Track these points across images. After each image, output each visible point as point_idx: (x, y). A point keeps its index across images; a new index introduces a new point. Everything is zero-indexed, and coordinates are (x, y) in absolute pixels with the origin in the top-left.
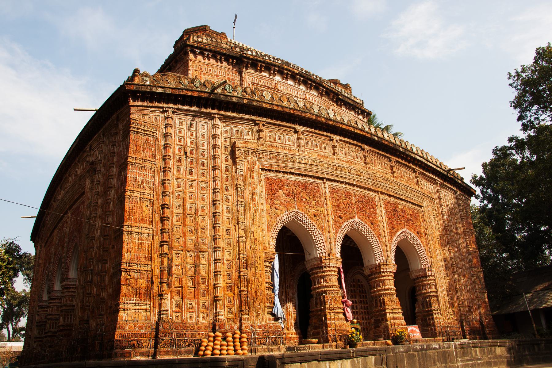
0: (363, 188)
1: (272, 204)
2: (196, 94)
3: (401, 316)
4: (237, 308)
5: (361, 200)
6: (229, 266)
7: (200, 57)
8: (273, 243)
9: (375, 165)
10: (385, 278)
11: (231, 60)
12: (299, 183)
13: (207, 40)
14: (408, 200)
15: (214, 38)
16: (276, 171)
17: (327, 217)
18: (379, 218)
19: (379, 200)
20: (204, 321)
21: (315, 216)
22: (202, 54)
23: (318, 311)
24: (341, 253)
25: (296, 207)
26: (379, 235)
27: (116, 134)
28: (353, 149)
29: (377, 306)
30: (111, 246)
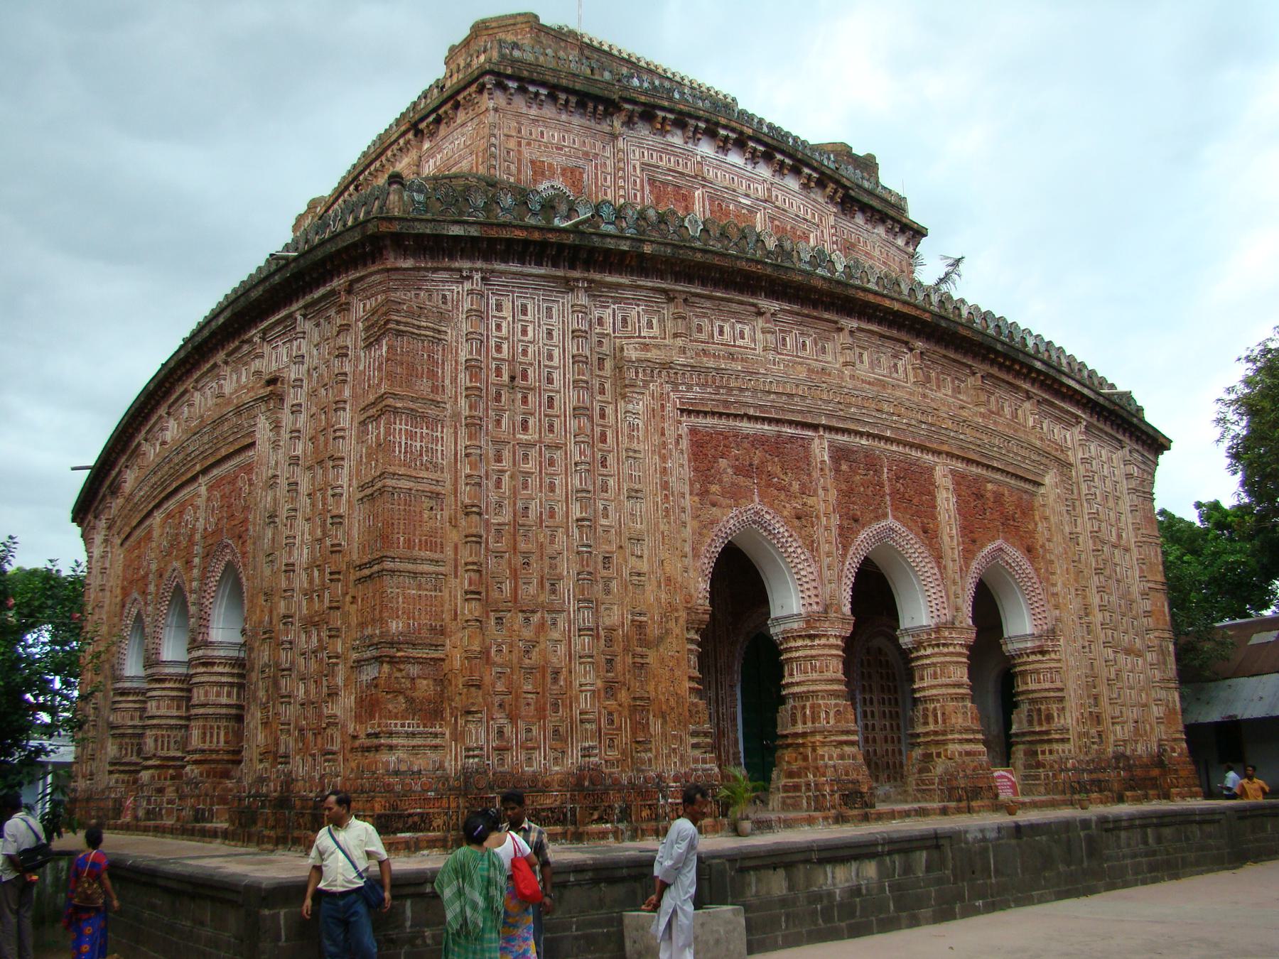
0: (905, 446)
1: (704, 493)
2: (536, 236)
3: (981, 747)
4: (625, 738)
6: (609, 641)
7: (520, 103)
8: (702, 587)
9: (939, 387)
10: (948, 659)
11: (591, 105)
16: (713, 414)
17: (824, 520)
18: (943, 517)
19: (942, 472)
20: (557, 768)
21: (799, 518)
22: (522, 90)
23: (796, 735)
24: (852, 603)
25: (757, 500)
26: (939, 558)
27: (345, 328)
28: (889, 348)
29: (926, 723)
30: (348, 598)
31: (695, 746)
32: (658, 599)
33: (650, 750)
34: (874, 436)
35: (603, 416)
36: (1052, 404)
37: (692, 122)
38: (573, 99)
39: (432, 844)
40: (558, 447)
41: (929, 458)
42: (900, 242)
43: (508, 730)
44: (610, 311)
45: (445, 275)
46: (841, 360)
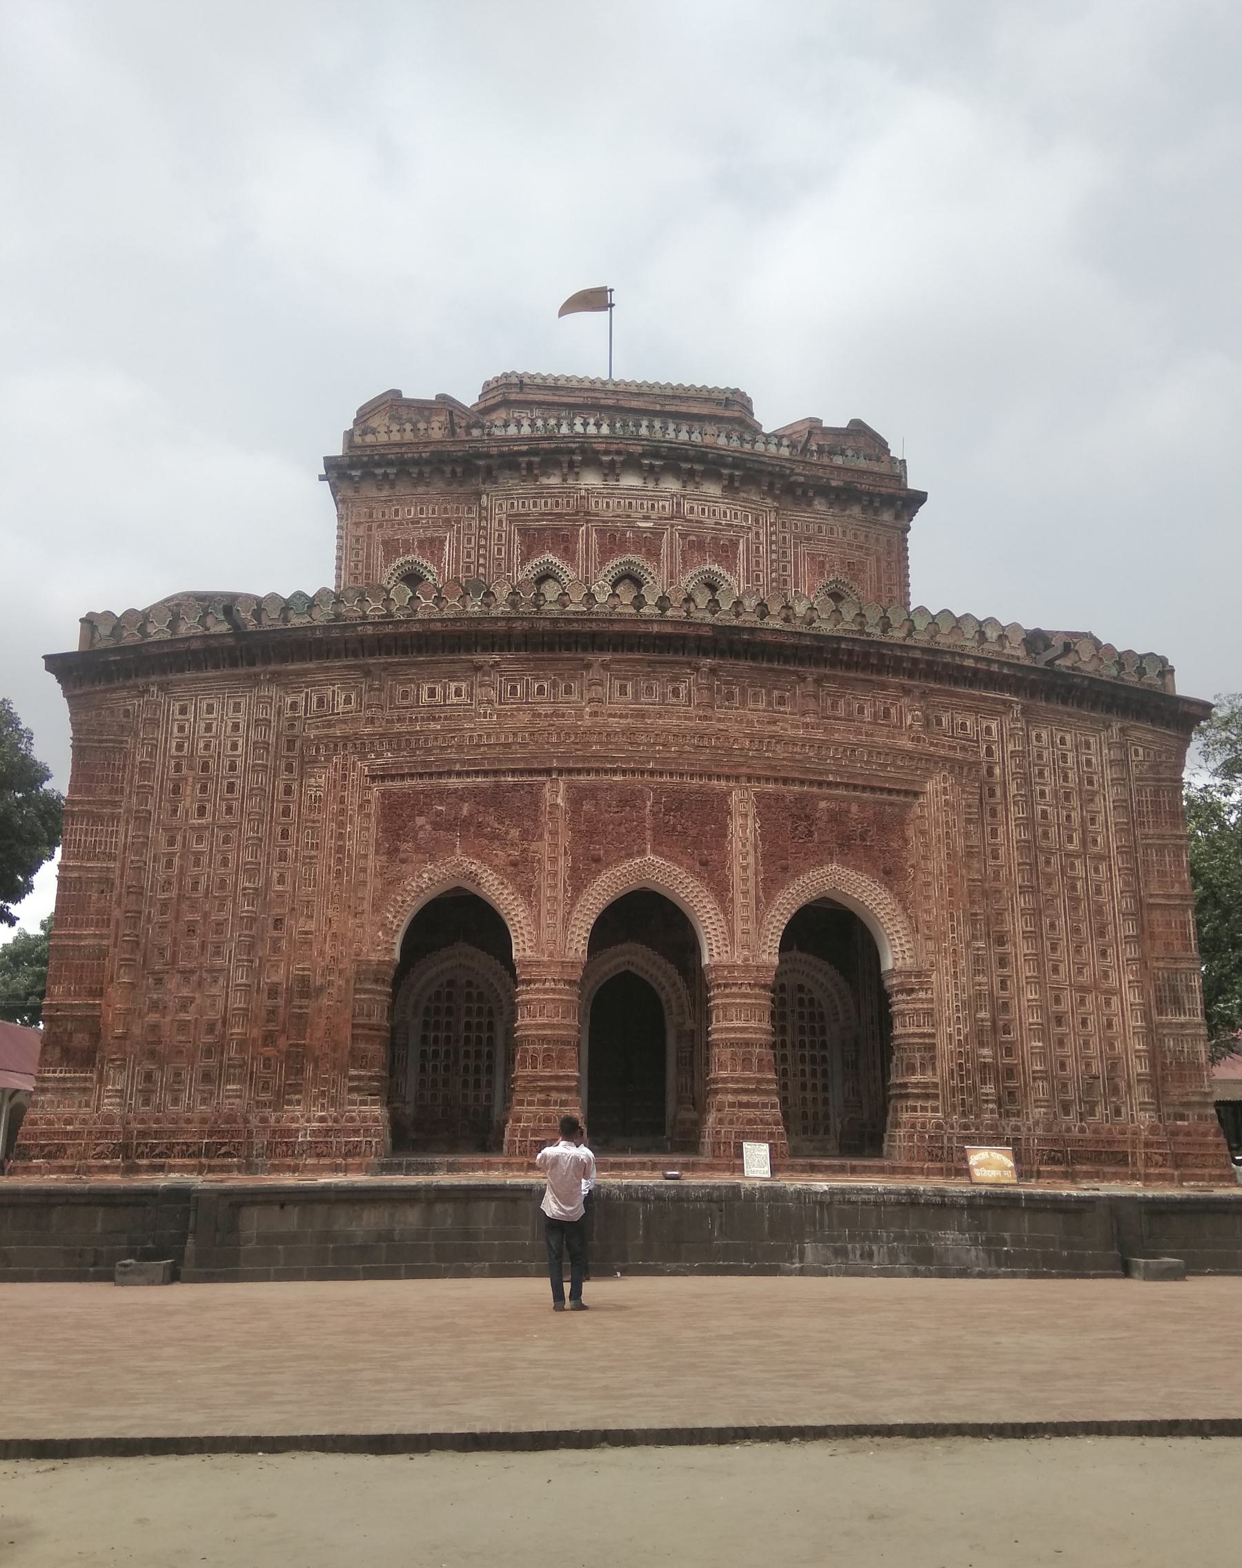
1: (393, 852)
3: (776, 1100)
5: (676, 803)
12: (474, 794)
13: (389, 432)
14: (859, 782)
15: (410, 421)
16: (412, 776)
17: (548, 866)
18: (737, 846)
22: (368, 475)
25: (458, 851)
26: (721, 890)
31: (351, 1090)
32: (322, 953)
33: (300, 1092)
34: (633, 772)
35: (288, 791)
37: (565, 458)
38: (427, 469)
39: (63, 1169)
40: (233, 827)
42: (887, 516)
43: (157, 1075)
44: (303, 695)
46: (587, 697)
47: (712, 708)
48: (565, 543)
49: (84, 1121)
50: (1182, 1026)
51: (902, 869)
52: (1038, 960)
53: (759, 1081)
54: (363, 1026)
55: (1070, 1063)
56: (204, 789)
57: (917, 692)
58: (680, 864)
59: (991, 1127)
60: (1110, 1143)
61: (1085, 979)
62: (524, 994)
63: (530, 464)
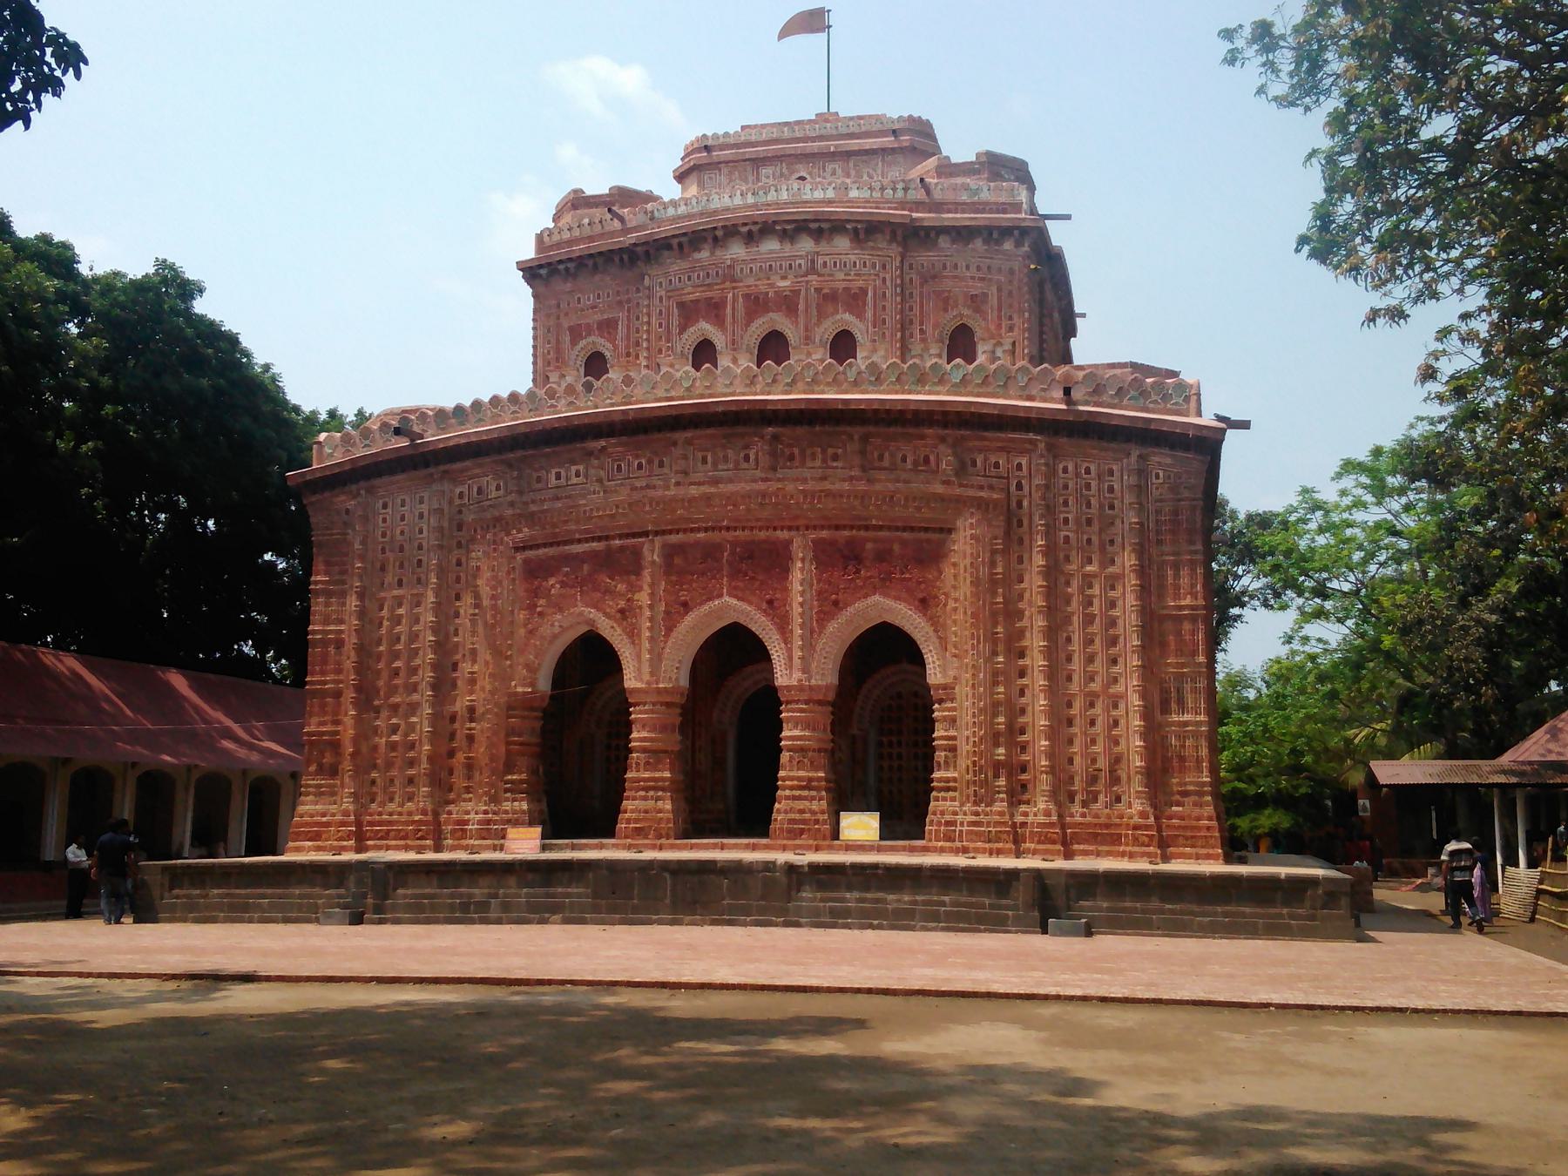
1: (532, 607)
12: (594, 555)
16: (545, 545)
17: (648, 613)
18: (796, 587)
26: (783, 627)
31: (506, 791)
32: (483, 689)
34: (713, 529)
35: (459, 564)
36: (985, 439)
41: (783, 535)
42: (1008, 246)
45: (343, 498)
47: (774, 469)
48: (714, 310)
49: (333, 815)
50: (1186, 724)
51: (936, 597)
52: (1052, 673)
53: (810, 780)
54: (515, 743)
55: (1077, 760)
56: (402, 566)
57: (950, 440)
58: (750, 603)
59: (1001, 814)
60: (1107, 826)
61: (1095, 686)
62: (636, 715)
63: (680, 245)
